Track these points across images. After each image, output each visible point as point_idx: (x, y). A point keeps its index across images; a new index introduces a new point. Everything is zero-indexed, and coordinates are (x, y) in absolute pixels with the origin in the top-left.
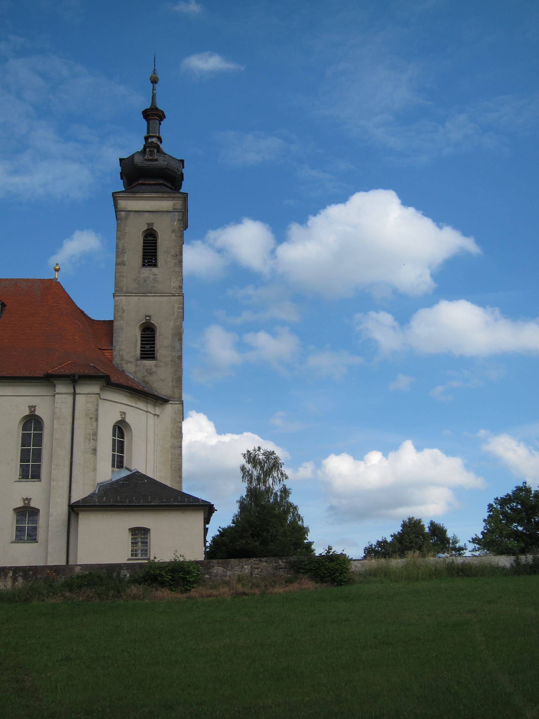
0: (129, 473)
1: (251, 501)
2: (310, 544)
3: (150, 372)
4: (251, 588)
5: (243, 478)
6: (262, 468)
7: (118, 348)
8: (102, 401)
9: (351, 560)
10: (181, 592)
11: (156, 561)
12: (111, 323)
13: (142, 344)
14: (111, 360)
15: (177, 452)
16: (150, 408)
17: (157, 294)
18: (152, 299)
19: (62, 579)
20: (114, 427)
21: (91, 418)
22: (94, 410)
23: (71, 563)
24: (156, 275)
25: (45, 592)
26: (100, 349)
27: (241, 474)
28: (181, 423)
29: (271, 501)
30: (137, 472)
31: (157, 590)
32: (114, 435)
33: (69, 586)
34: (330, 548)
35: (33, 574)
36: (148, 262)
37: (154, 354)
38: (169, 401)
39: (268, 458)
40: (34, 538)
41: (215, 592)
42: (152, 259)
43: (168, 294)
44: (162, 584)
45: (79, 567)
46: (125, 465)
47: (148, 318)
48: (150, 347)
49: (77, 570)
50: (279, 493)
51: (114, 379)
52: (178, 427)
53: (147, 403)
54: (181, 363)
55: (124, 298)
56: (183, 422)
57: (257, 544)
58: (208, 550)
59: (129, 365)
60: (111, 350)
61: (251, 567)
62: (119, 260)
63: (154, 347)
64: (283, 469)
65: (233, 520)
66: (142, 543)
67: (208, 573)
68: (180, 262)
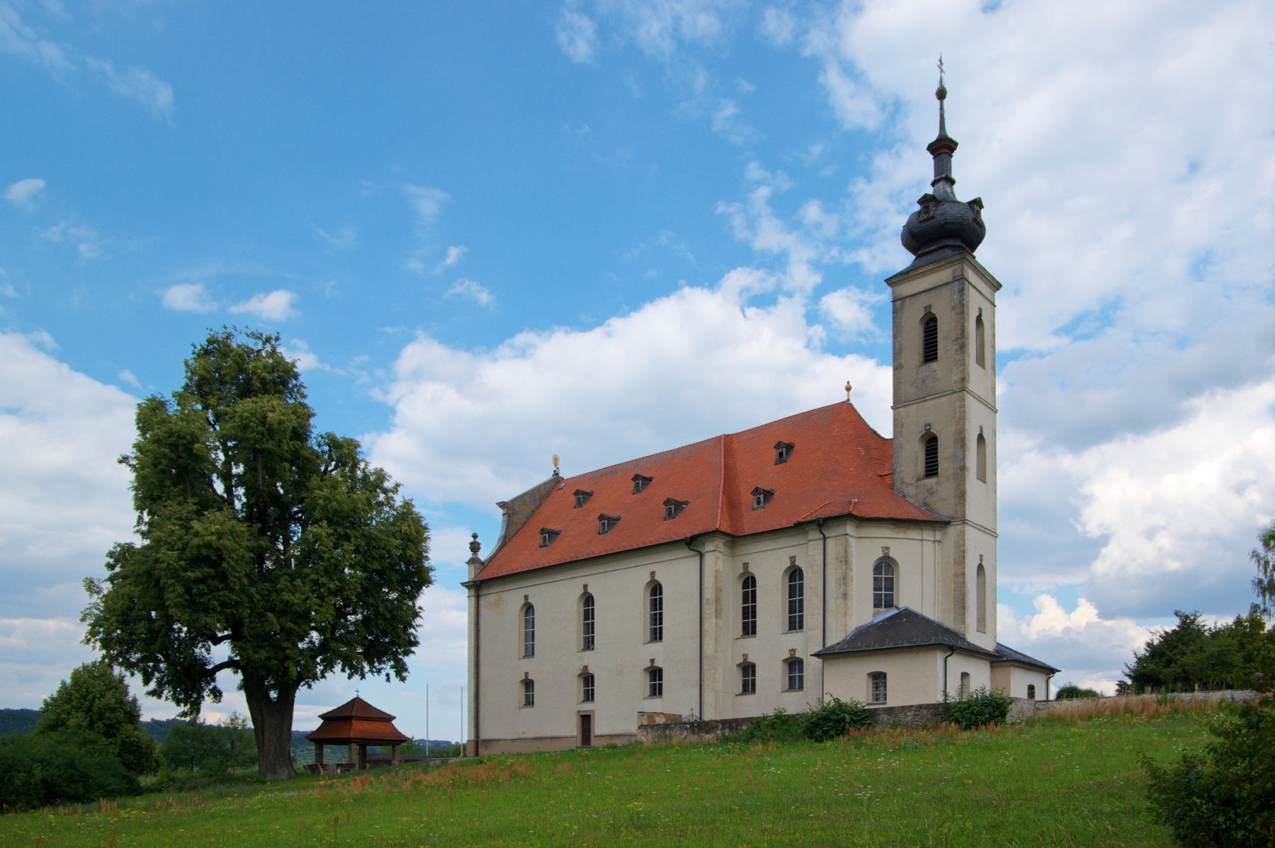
3: (931, 492)
7: (898, 470)
15: (961, 579)
17: (937, 396)
43: (948, 393)
52: (961, 551)
55: (902, 409)
59: (910, 488)
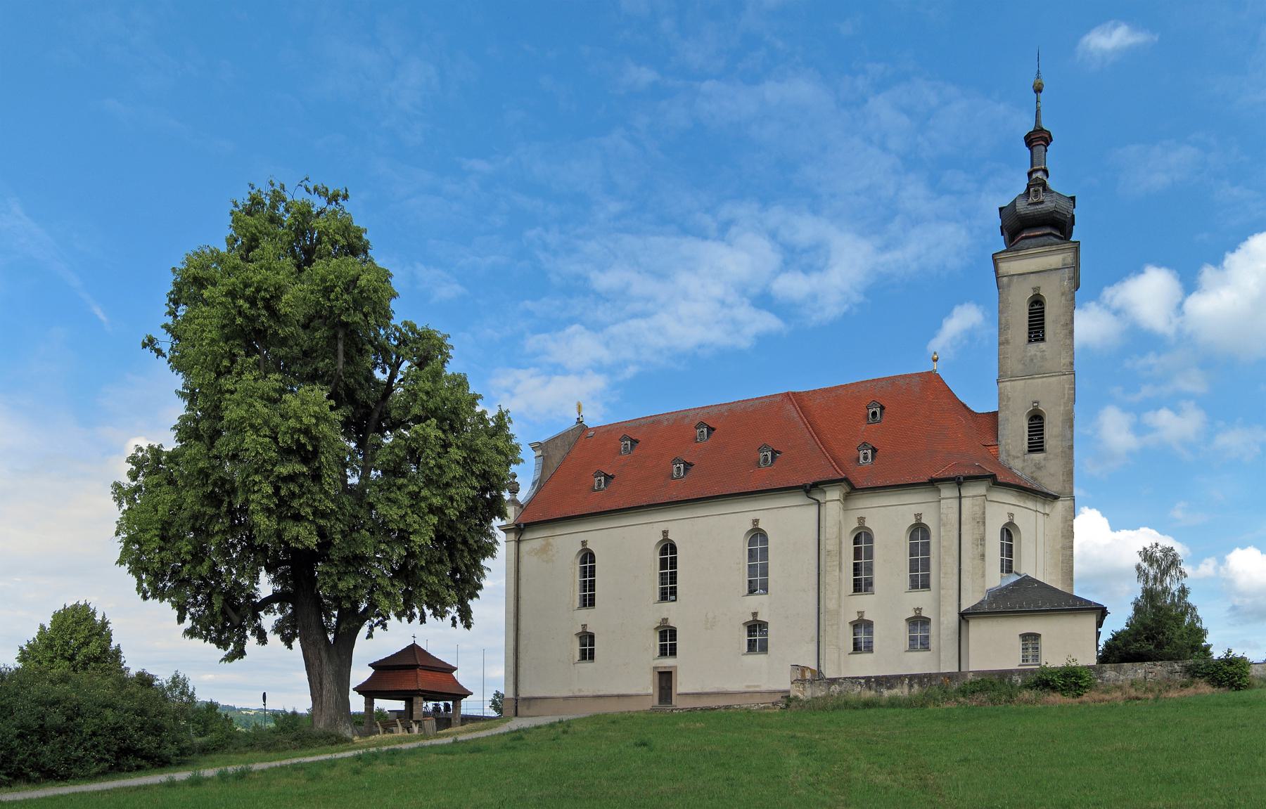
0: (1019, 578)
2: (1208, 647)
3: (1039, 467)
4: (1145, 693)
6: (1159, 566)
7: (1003, 442)
9: (1252, 663)
10: (1073, 697)
11: (1048, 666)
12: (995, 414)
13: (1029, 435)
14: (997, 457)
15: (1068, 553)
16: (1040, 507)
17: (1047, 375)
18: (1040, 381)
19: (956, 686)
20: (1003, 529)
21: (978, 522)
24: (1044, 351)
25: (940, 697)
27: (1136, 574)
29: (1168, 602)
30: (1027, 576)
31: (1049, 695)
32: (1002, 539)
33: (963, 692)
34: (1230, 651)
35: (928, 681)
36: (1035, 336)
37: (1043, 446)
38: (1059, 497)
39: (1166, 556)
40: (926, 646)
41: (1107, 697)
42: (1039, 332)
43: (1057, 374)
44: (1054, 689)
45: (971, 674)
46: (1014, 569)
47: (1035, 404)
49: (970, 676)
50: (1176, 593)
51: (1000, 478)
53: (1036, 501)
55: (1009, 383)
56: (1074, 520)
57: (1152, 647)
58: (1100, 654)
59: (1016, 460)
61: (1145, 671)
62: (1003, 338)
63: (1043, 438)
64: (1182, 566)
65: (1127, 623)
66: (1033, 648)
67: (1100, 678)
68: (1072, 332)
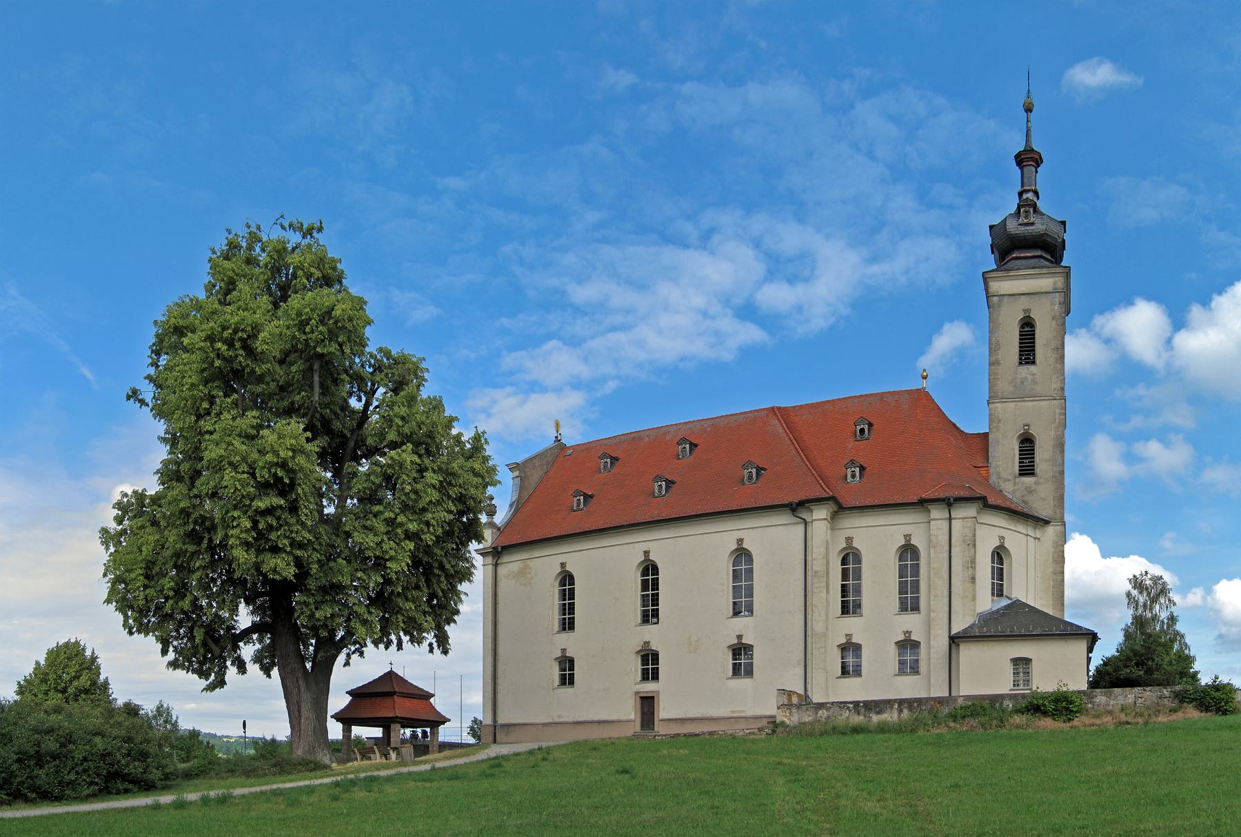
0: (1010, 602)
1: (1137, 629)
2: (1196, 673)
5: (1128, 604)
6: (1149, 594)
7: (994, 464)
8: (979, 525)
12: (986, 435)
13: (1020, 459)
16: (1030, 531)
18: (1030, 404)
19: (946, 710)
20: (993, 553)
21: (969, 545)
22: (971, 535)
23: (953, 694)
24: (1034, 374)
25: (930, 722)
26: (976, 467)
27: (1126, 601)
28: (1063, 546)
29: (1158, 628)
30: (1018, 600)
31: (1040, 719)
32: (993, 562)
33: (954, 717)
34: (1217, 678)
36: (1025, 359)
37: (1033, 470)
38: (1050, 522)
40: (916, 670)
41: (1097, 721)
42: (1029, 355)
44: (1045, 713)
46: (1005, 593)
47: (1026, 428)
48: (1029, 462)
49: (960, 701)
50: (1166, 621)
51: (991, 501)
54: (1063, 479)
57: (1142, 673)
58: (1091, 679)
60: (987, 467)
62: (993, 359)
63: (1033, 462)
64: (1171, 595)
65: (1117, 649)
66: (1024, 673)
68: (1062, 357)
